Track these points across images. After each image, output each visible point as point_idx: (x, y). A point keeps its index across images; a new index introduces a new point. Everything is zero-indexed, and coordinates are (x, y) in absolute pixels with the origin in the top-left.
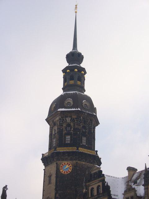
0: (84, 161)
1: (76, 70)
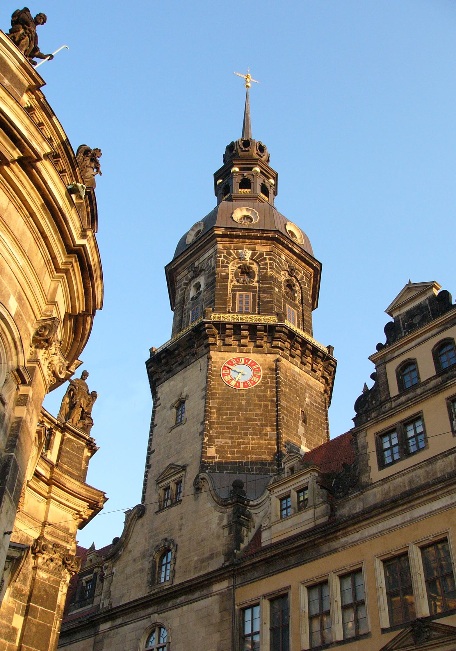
0: (296, 365)
1: (258, 169)
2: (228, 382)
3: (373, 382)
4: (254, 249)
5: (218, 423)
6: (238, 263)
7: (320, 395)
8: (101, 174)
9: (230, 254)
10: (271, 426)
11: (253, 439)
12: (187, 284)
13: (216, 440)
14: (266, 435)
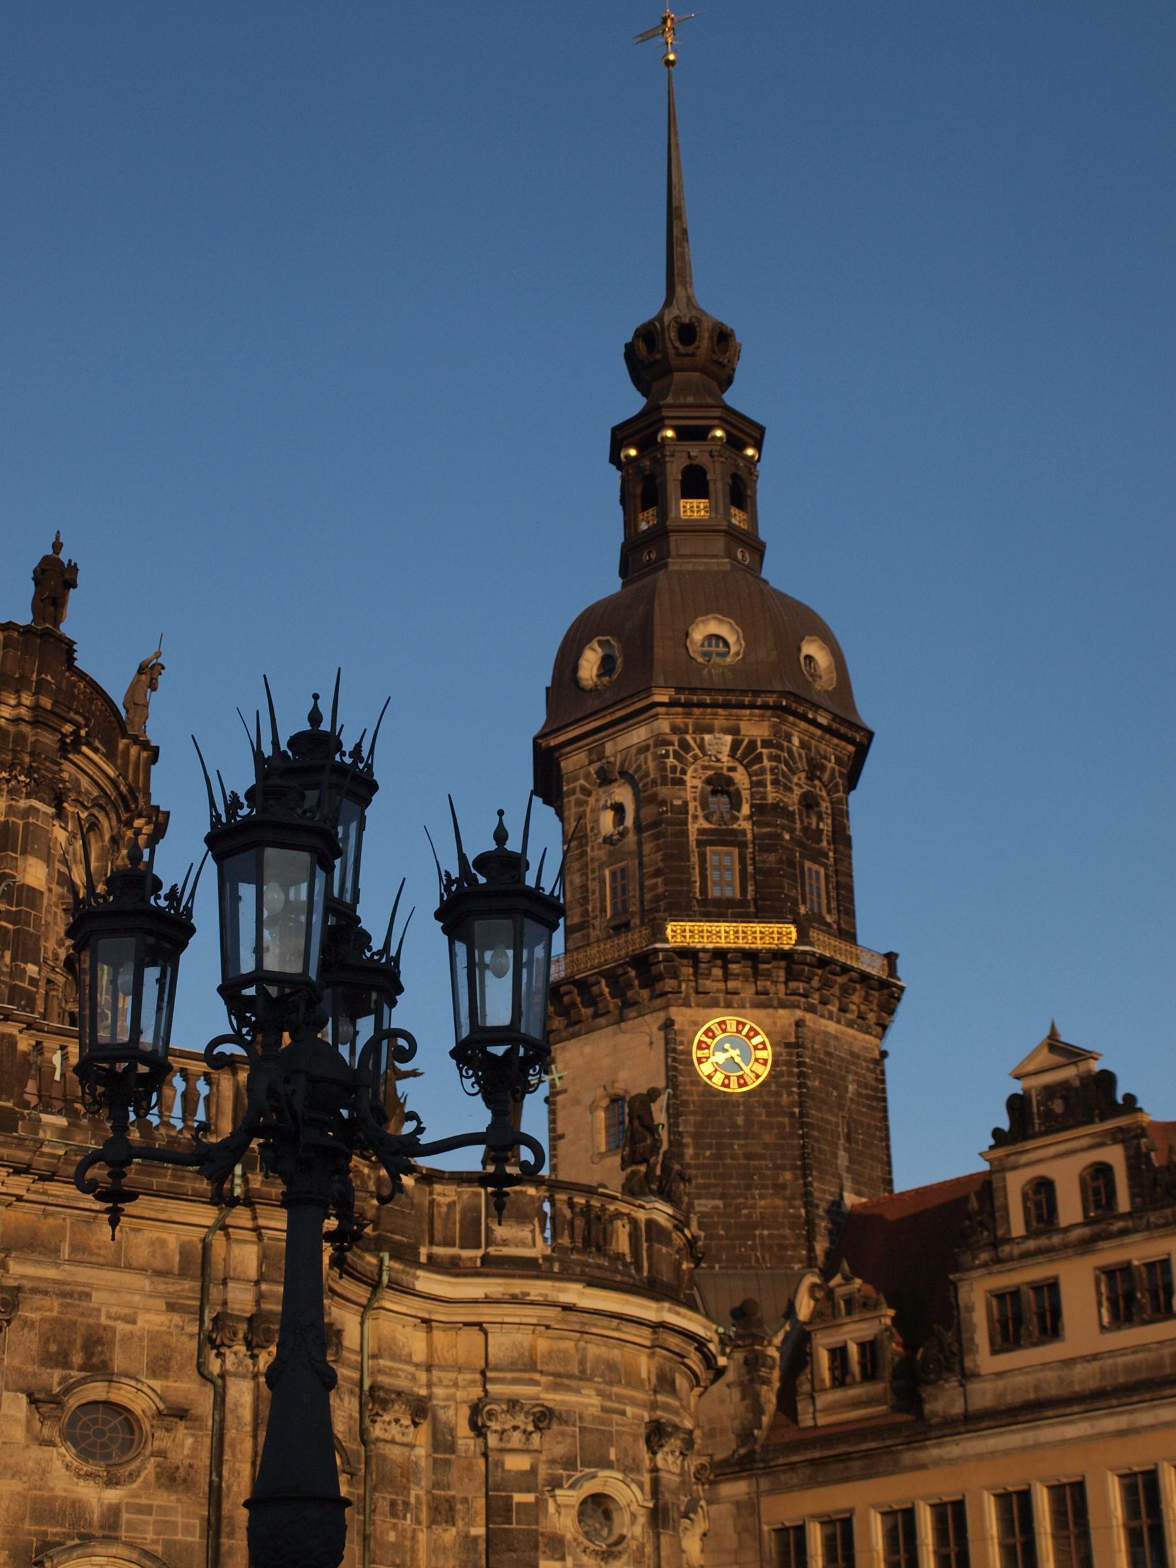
0: (830, 1018)
2: (710, 1077)
4: (735, 731)
5: (697, 1167)
6: (705, 768)
7: (872, 1066)
10: (794, 1167)
11: (762, 1197)
14: (783, 1187)
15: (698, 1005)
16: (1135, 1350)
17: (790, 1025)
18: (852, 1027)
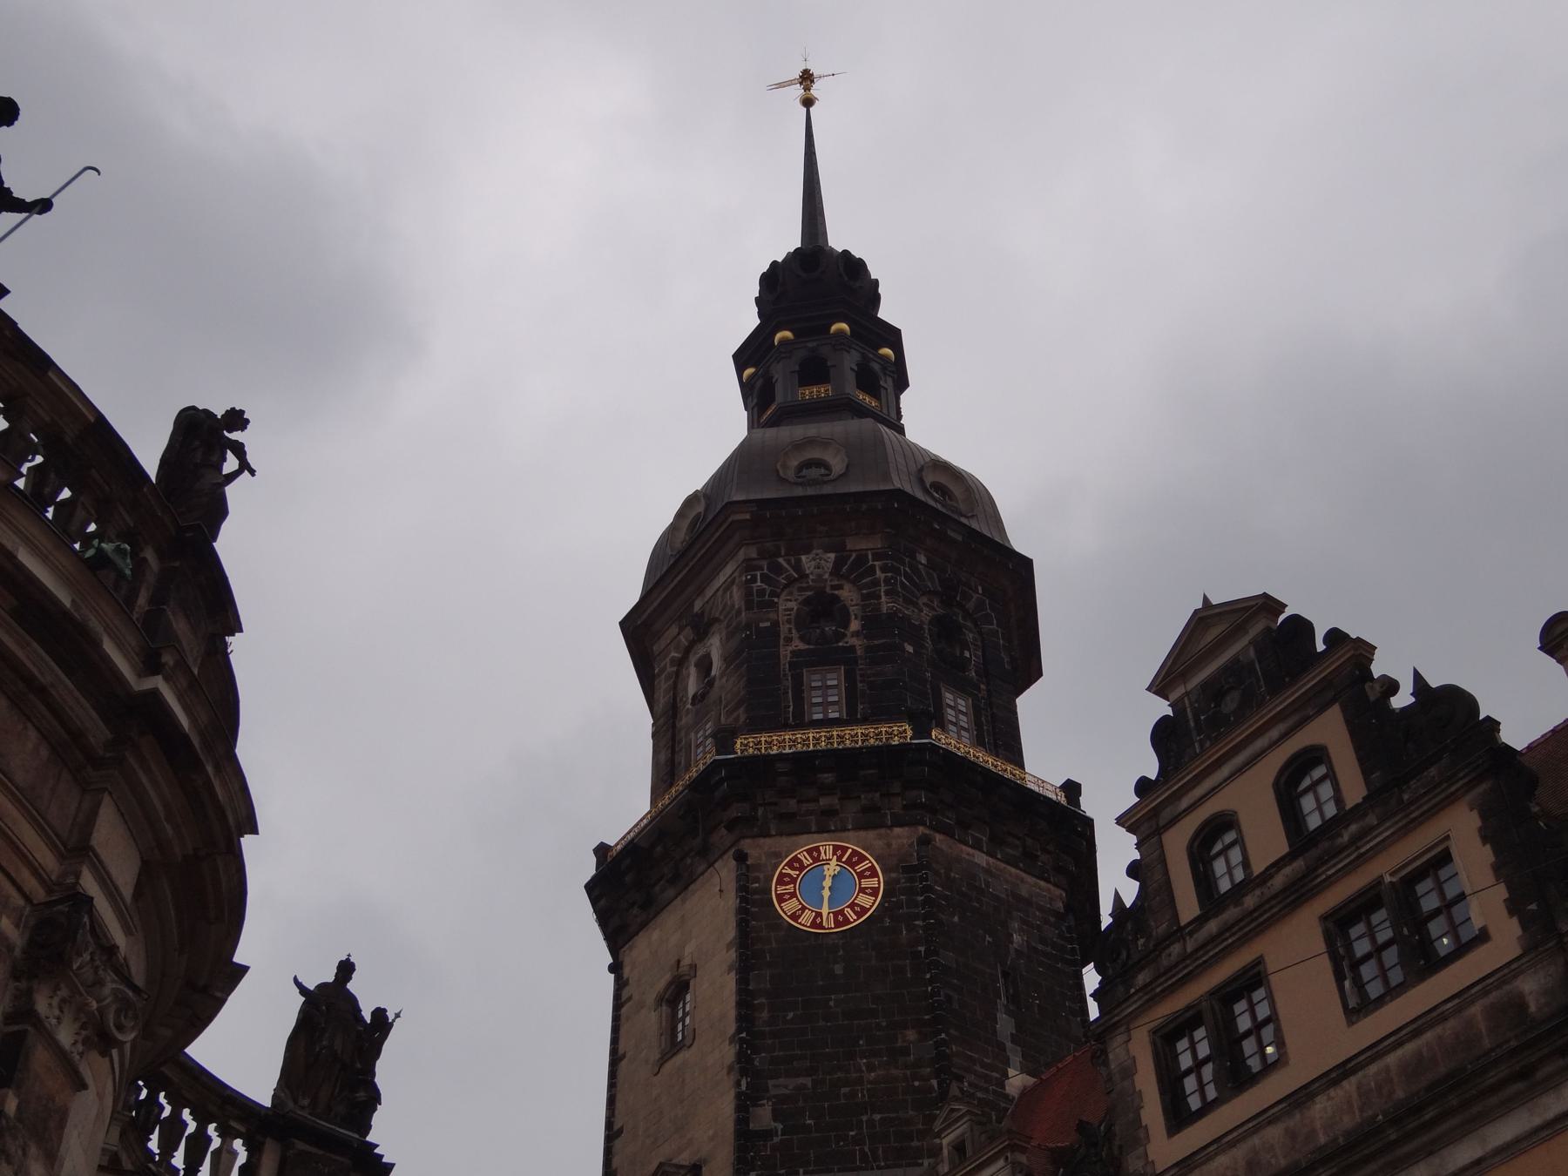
0: (977, 846)
2: (795, 917)
3: (1134, 886)
8: (252, 472)
9: (778, 569)
11: (871, 1068)
12: (681, 663)
13: (771, 1083)
14: (905, 1052)
15: (781, 834)
16: (1416, 1028)
17: (911, 845)
18: (1017, 867)
